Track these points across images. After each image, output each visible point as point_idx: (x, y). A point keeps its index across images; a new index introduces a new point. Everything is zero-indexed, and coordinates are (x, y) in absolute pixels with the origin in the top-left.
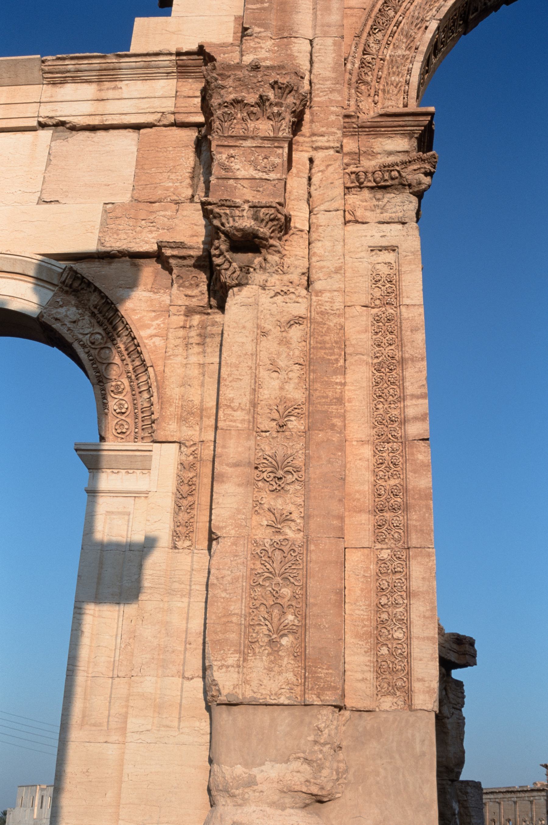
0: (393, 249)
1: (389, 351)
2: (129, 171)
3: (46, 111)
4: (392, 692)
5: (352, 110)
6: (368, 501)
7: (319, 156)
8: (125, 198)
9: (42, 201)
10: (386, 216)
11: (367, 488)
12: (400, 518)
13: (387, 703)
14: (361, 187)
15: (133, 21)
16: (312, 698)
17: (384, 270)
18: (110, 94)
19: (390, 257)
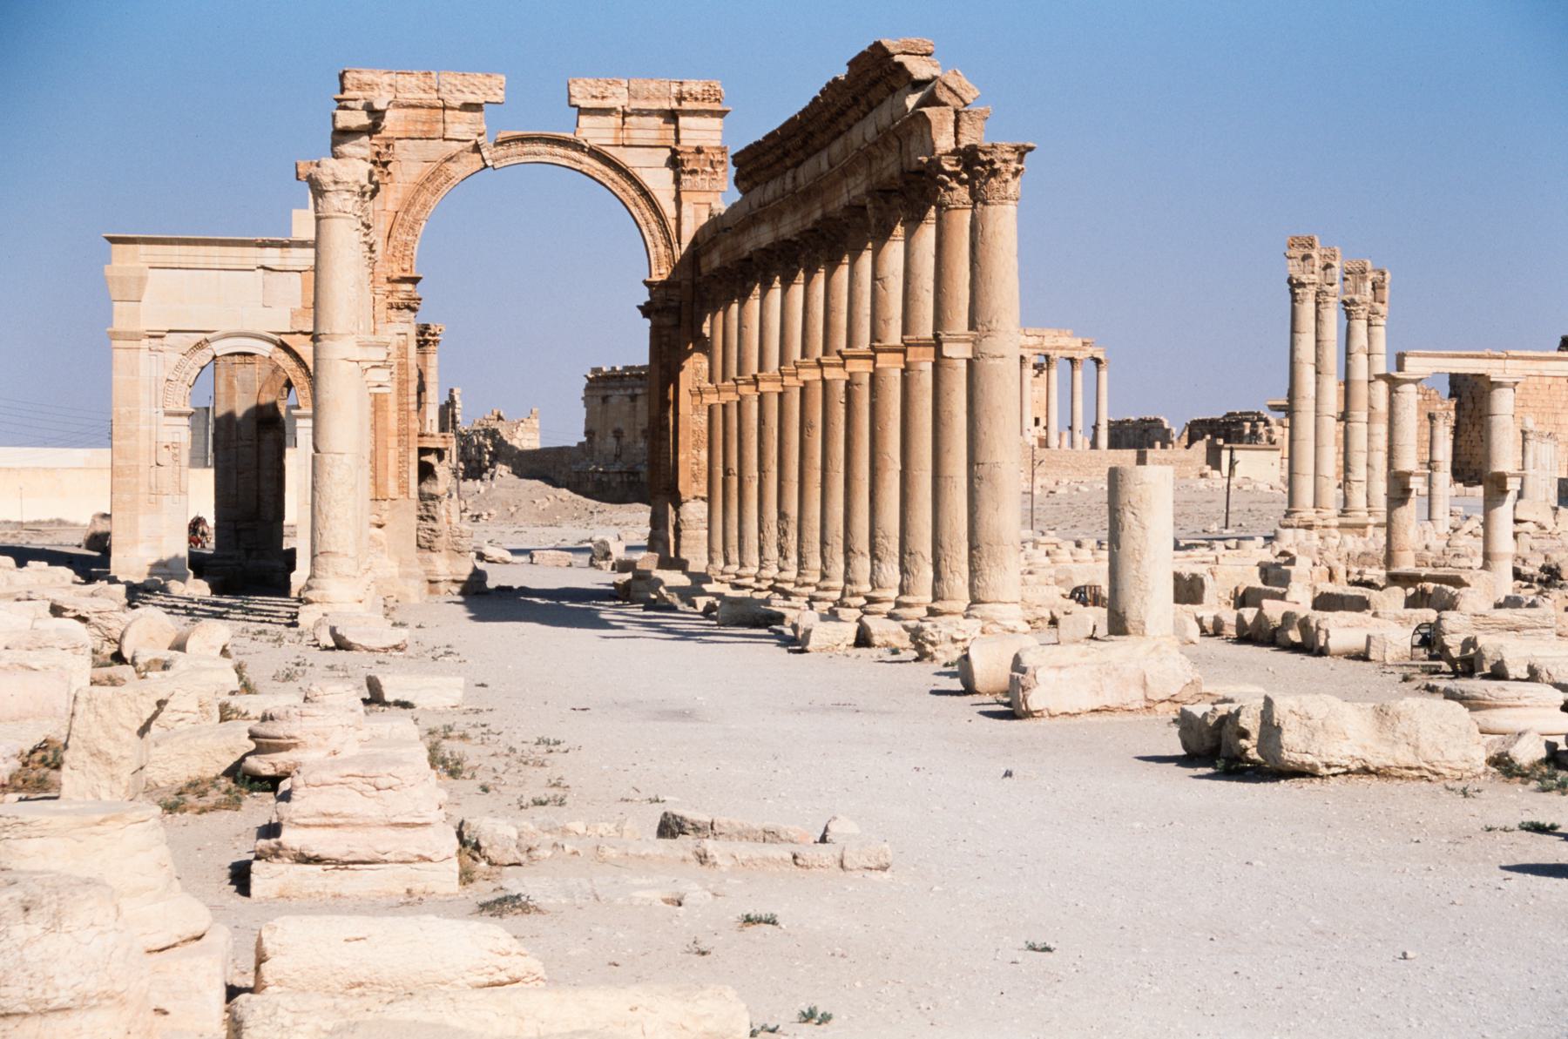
0: (405, 334)
1: (404, 377)
2: (299, 293)
3: (260, 262)
4: (403, 493)
5: (389, 275)
6: (396, 432)
7: (377, 297)
8: (299, 306)
9: (264, 306)
10: (403, 319)
11: (395, 428)
12: (406, 438)
13: (402, 496)
14: (392, 308)
15: (291, 212)
16: (379, 497)
17: (402, 343)
18: (287, 255)
19: (403, 337)
